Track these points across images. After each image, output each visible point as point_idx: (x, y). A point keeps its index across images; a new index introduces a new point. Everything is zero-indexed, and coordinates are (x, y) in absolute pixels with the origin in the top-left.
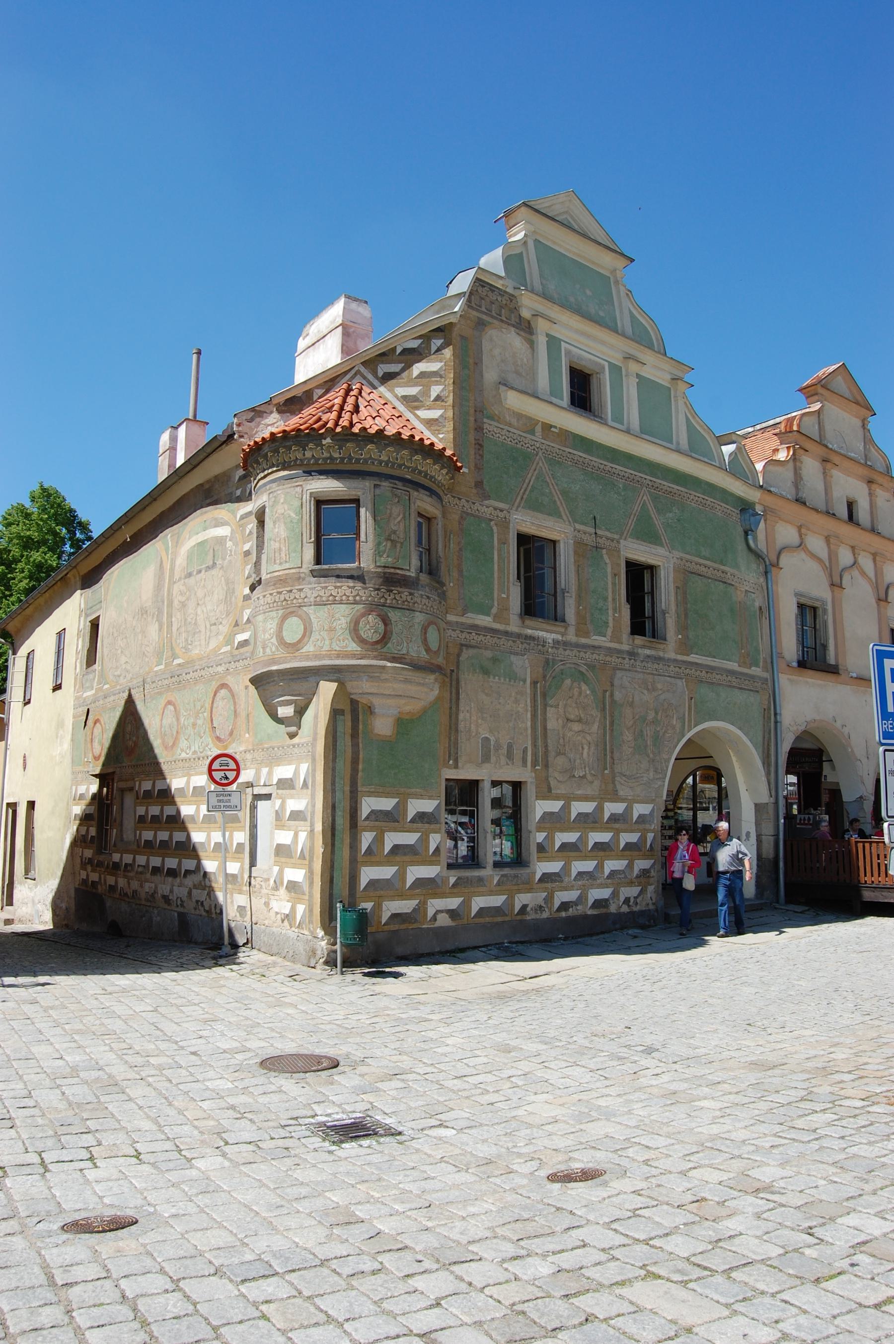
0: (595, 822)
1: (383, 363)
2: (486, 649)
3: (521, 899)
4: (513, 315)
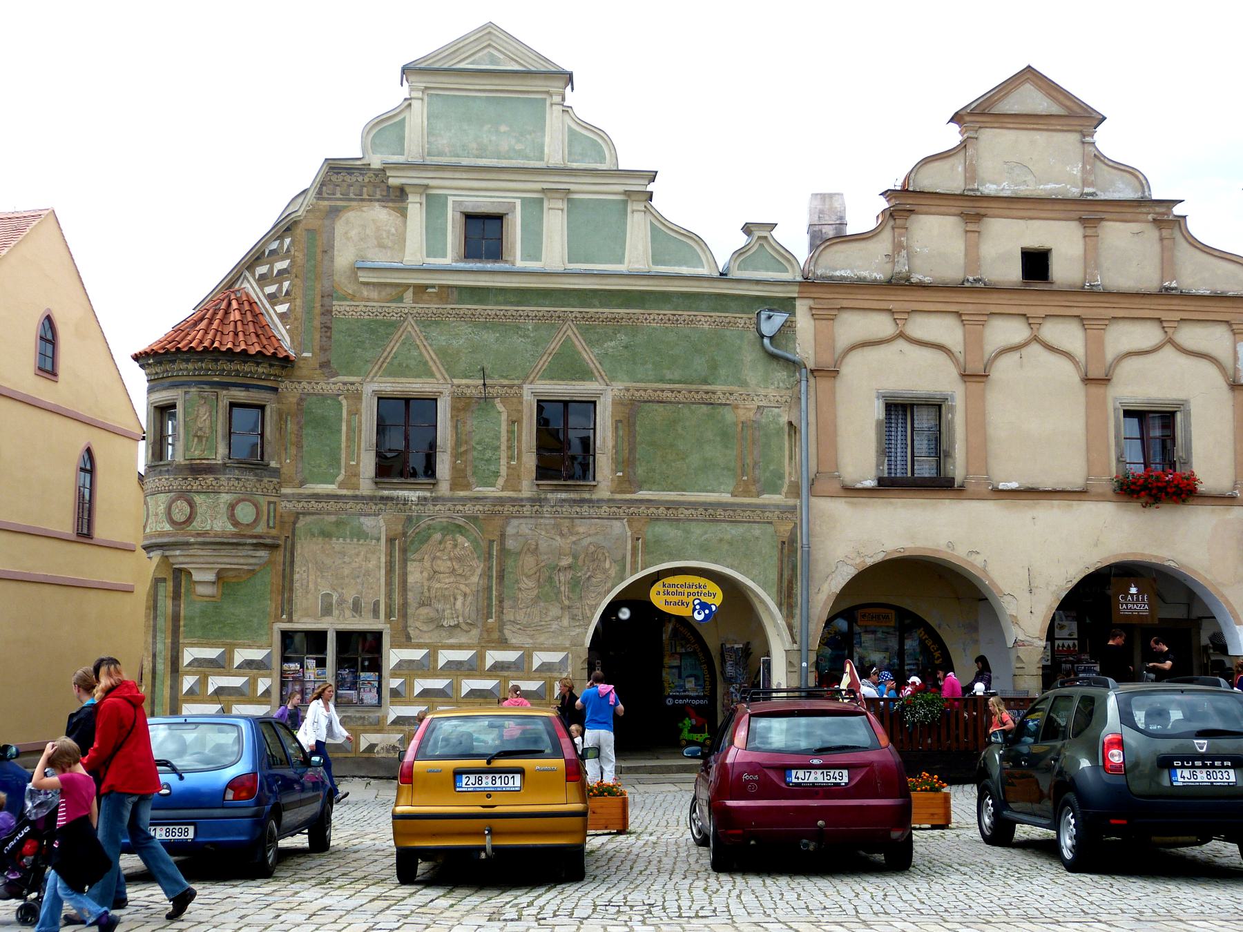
0: (473, 670)
2: (329, 514)
3: (365, 741)
4: (378, 190)
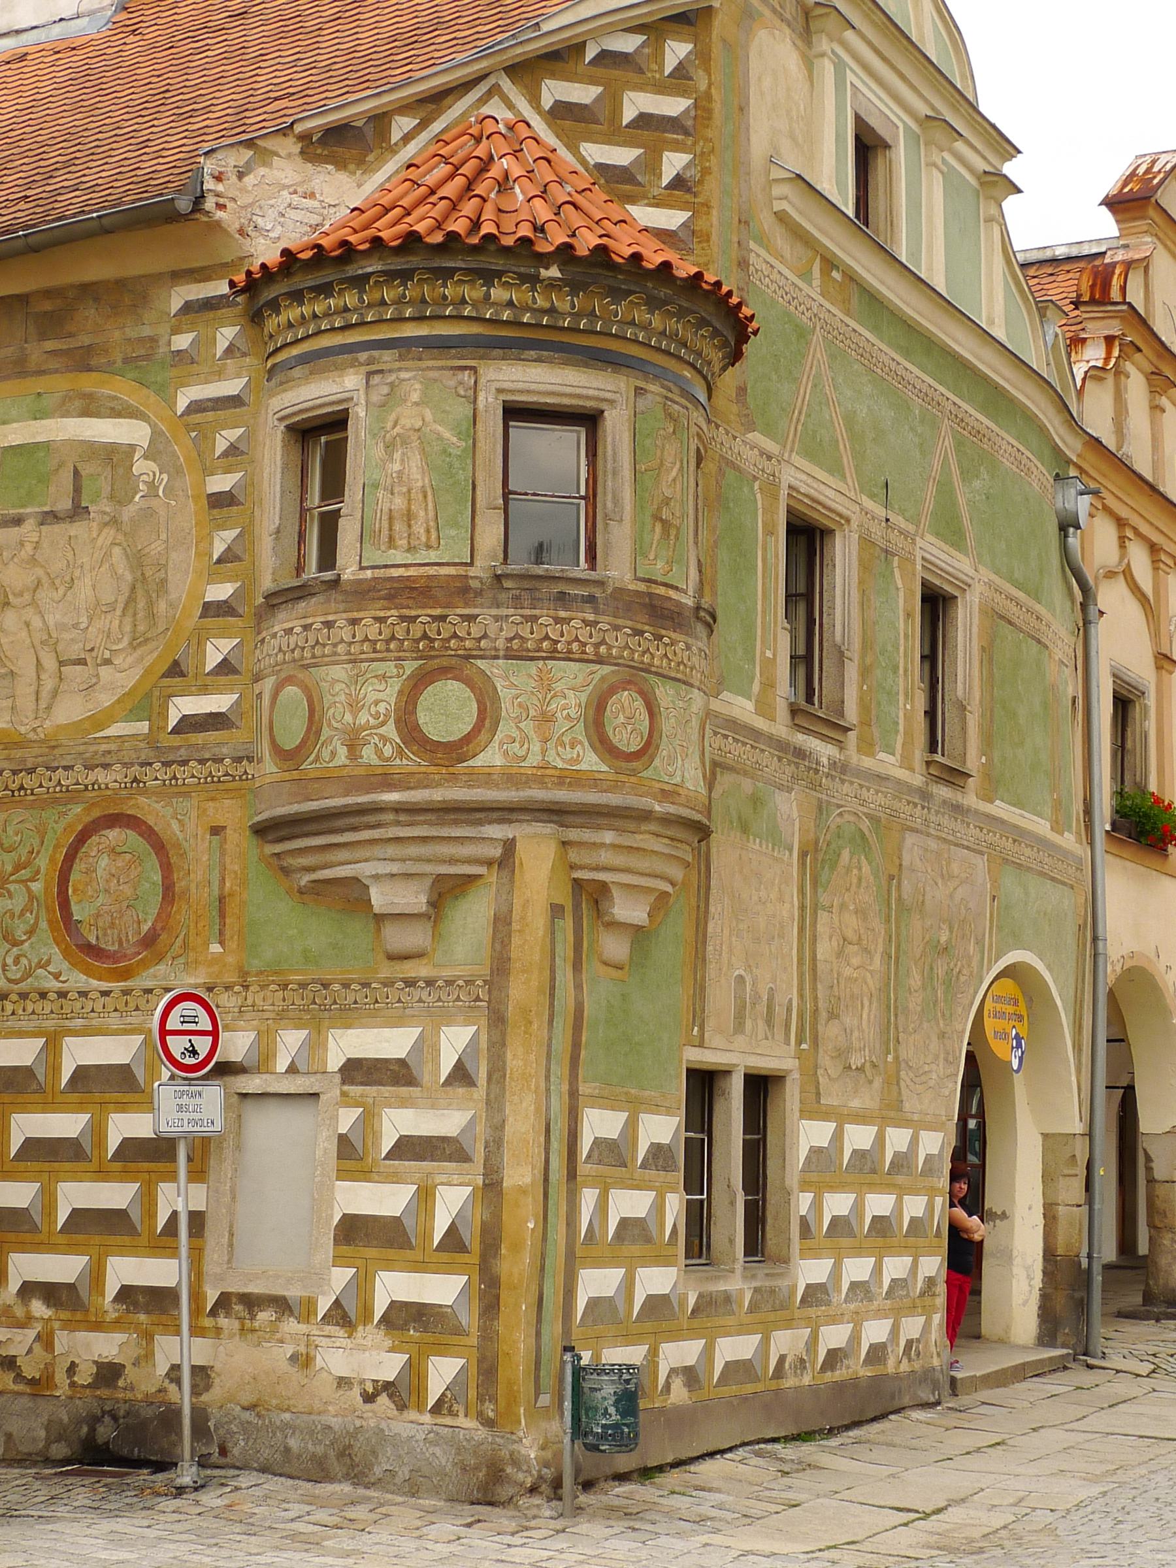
1: (553, 76)
2: (745, 774)
